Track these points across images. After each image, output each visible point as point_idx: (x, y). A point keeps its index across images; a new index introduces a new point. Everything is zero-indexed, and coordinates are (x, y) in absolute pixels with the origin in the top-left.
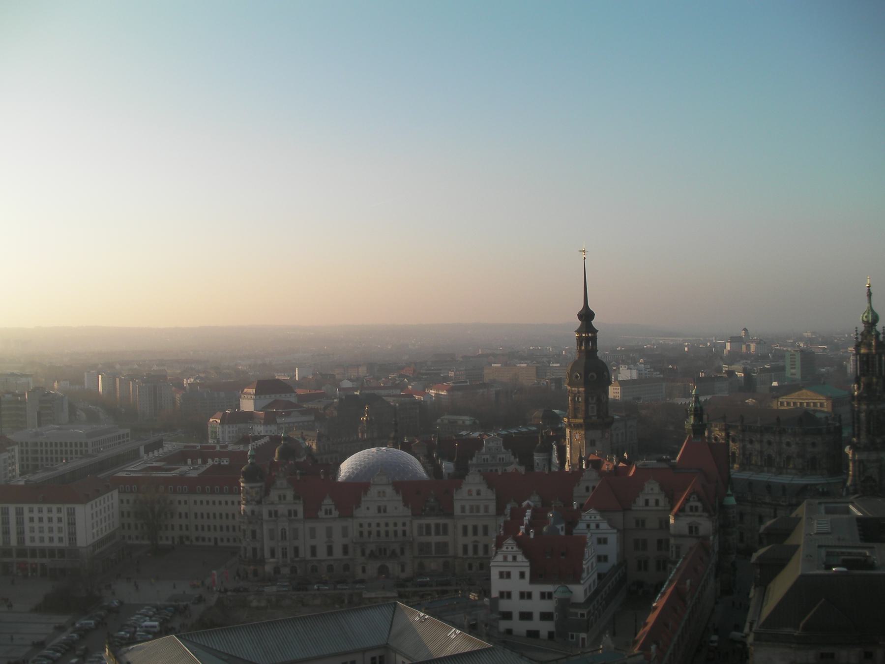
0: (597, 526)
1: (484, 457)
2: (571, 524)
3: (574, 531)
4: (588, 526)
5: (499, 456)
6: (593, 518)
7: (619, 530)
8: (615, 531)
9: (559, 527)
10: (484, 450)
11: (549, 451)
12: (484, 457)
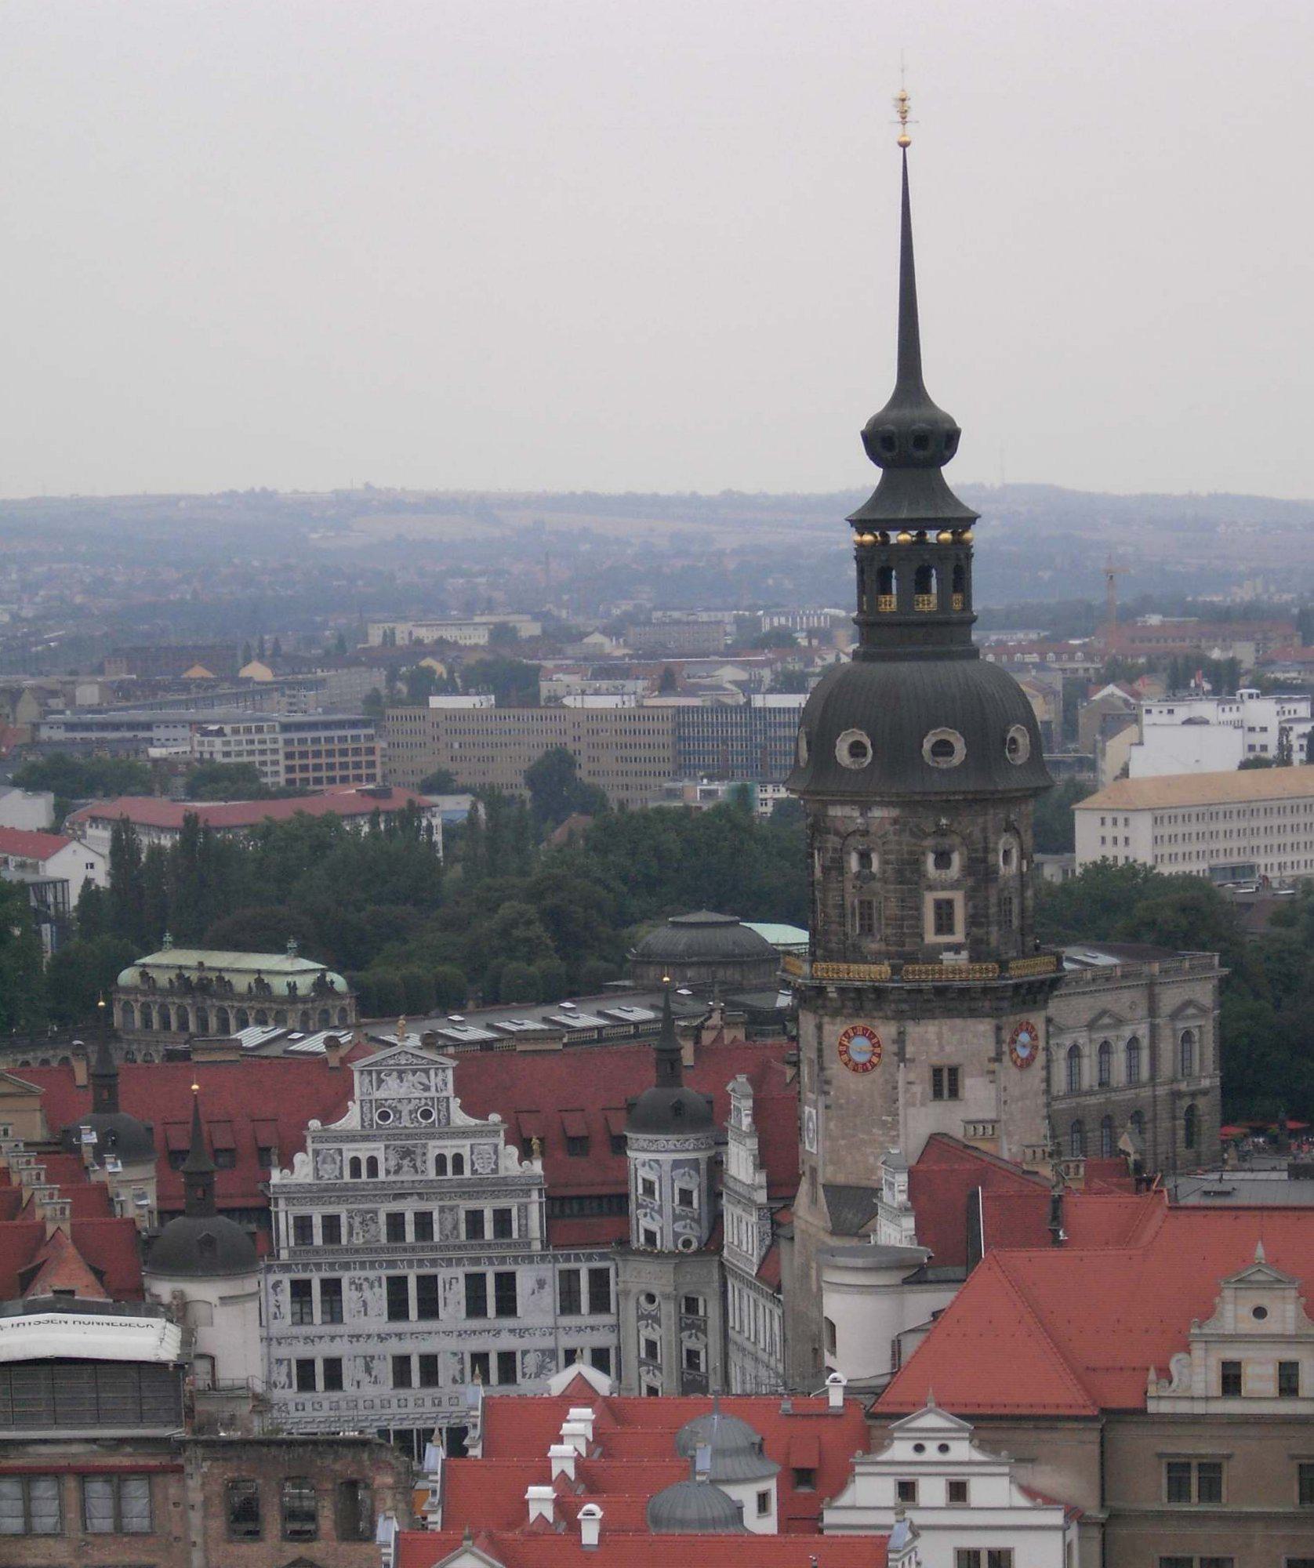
0: (958, 1491)
1: (350, 1151)
2: (809, 1483)
3: (830, 1517)
4: (907, 1490)
5: (434, 1148)
6: (932, 1452)
7: (1074, 1514)
8: (1056, 1518)
9: (746, 1495)
10: (351, 1120)
11: (703, 1120)
12: (350, 1151)
